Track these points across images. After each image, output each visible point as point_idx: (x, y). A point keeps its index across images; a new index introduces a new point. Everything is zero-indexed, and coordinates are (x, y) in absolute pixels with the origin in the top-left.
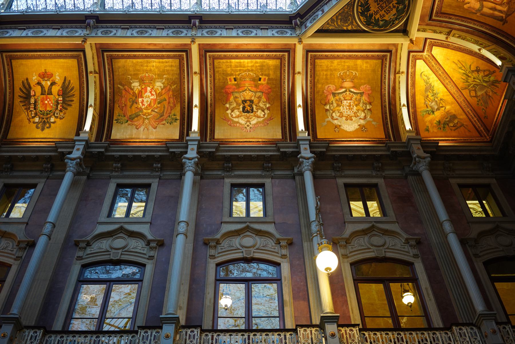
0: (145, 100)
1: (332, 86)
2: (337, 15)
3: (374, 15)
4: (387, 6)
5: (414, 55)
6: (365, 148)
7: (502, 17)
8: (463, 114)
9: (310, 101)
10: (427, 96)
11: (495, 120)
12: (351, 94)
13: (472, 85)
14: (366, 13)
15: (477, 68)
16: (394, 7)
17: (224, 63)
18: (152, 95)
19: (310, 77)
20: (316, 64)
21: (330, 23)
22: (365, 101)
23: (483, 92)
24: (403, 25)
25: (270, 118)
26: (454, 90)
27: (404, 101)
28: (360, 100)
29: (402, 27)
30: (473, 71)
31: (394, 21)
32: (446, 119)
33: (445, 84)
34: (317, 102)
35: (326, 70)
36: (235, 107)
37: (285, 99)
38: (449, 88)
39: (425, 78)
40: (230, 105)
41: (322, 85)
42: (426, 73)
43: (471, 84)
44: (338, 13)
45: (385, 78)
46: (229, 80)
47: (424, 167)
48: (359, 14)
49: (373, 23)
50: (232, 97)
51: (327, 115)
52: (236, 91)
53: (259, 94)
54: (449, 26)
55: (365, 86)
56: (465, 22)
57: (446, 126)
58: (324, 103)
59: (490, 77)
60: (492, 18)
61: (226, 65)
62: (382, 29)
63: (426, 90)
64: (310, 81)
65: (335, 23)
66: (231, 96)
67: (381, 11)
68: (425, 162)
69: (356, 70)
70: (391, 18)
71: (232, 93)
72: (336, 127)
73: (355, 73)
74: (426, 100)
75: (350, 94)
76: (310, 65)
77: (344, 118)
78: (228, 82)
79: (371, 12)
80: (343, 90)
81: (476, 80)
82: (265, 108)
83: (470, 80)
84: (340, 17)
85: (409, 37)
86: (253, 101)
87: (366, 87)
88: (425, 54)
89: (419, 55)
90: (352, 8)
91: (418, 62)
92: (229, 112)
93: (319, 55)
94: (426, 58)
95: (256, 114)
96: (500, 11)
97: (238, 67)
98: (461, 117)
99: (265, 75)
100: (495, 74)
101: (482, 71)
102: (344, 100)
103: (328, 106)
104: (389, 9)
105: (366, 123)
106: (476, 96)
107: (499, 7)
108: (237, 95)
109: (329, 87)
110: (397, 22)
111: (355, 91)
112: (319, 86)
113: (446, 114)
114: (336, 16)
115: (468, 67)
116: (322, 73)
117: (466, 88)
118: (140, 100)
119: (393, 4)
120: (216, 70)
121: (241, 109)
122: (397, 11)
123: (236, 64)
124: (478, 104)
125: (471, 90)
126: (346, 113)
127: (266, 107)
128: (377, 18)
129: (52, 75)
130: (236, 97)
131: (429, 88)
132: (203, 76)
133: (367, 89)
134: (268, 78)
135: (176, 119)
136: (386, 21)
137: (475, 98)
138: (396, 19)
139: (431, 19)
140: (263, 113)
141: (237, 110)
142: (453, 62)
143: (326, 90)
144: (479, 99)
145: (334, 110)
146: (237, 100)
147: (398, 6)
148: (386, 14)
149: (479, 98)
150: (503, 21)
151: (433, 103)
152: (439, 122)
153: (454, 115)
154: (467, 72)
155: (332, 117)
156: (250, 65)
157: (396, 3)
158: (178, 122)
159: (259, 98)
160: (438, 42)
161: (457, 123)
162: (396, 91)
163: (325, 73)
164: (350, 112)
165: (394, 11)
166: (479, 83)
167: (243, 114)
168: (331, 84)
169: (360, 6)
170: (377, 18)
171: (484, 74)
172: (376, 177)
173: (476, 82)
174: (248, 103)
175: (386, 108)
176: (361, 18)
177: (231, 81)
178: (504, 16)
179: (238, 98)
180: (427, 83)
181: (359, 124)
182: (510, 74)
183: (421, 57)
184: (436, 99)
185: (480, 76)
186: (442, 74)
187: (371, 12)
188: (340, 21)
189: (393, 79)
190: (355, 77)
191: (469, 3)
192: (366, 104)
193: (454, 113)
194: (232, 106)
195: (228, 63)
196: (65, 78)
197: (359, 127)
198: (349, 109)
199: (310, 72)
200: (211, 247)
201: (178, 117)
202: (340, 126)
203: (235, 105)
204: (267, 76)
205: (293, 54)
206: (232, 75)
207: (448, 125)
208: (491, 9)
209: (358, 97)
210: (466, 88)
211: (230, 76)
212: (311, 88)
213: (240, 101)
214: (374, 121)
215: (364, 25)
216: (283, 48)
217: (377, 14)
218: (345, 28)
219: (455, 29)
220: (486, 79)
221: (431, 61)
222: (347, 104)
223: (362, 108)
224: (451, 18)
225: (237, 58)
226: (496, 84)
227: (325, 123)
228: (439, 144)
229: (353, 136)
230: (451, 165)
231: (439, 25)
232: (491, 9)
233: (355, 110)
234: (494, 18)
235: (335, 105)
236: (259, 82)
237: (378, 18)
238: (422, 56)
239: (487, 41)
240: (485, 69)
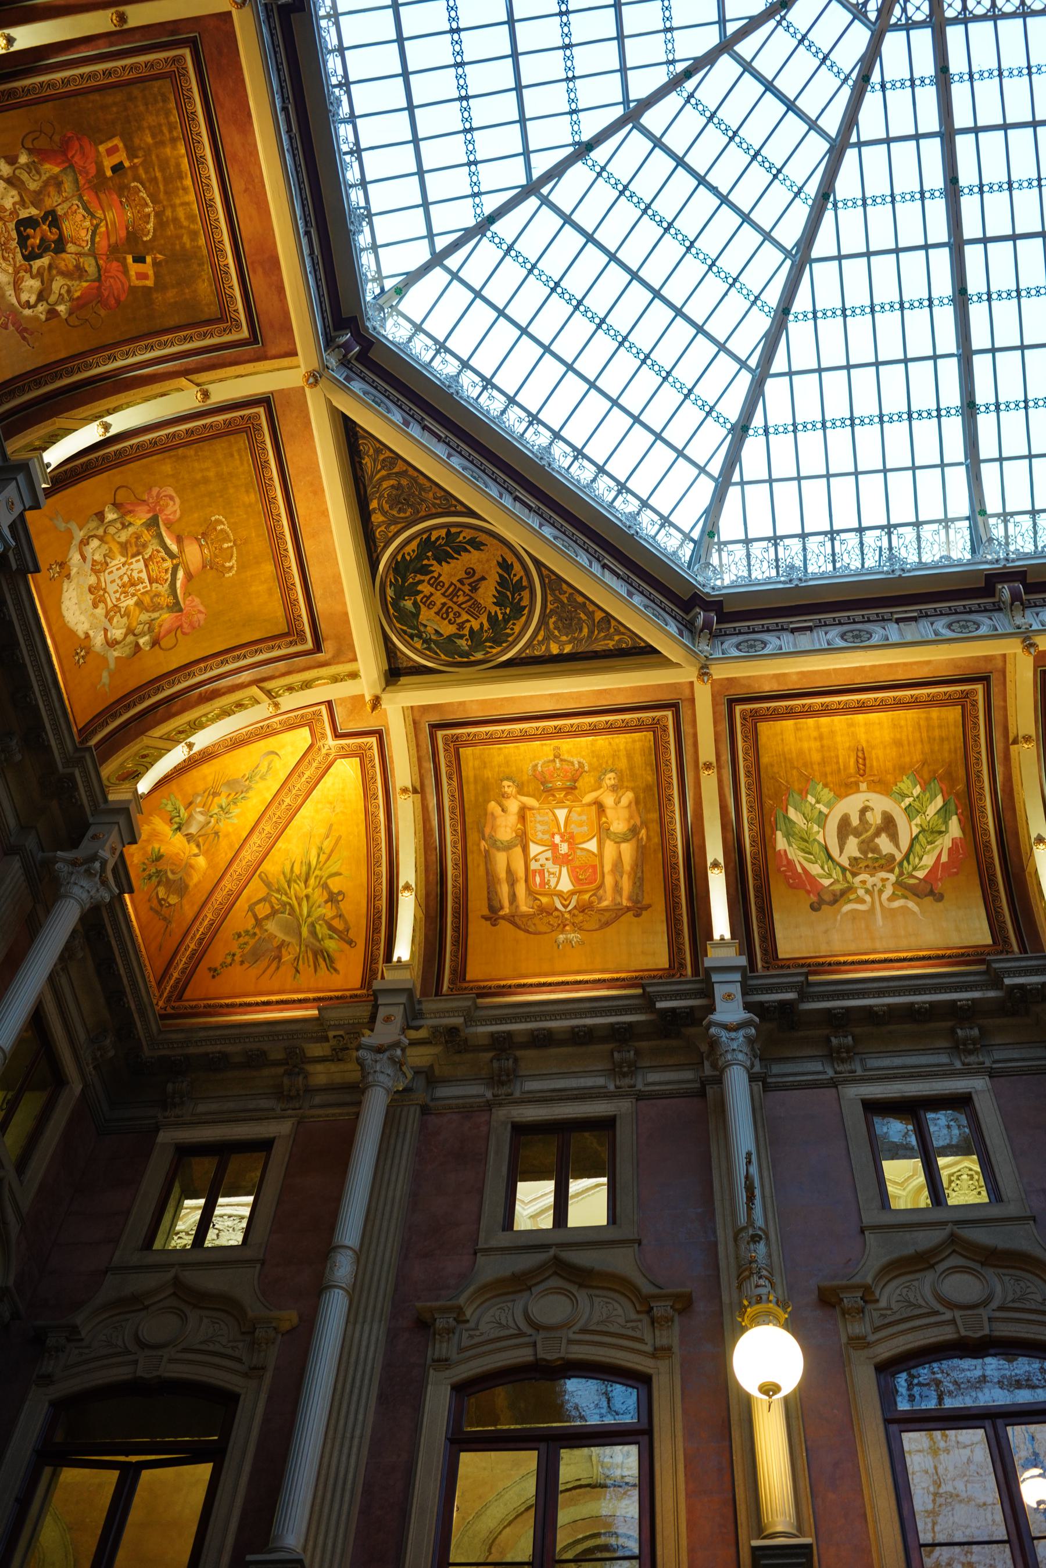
1: (177, 507)
2: (411, 471)
3: (427, 578)
4: (459, 606)
5: (320, 714)
6: (53, 691)
7: (502, 908)
8: (196, 908)
9: (115, 452)
10: (216, 794)
11: (222, 1001)
12: (169, 576)
13: (284, 898)
14: (430, 554)
15: (340, 893)
16: (461, 626)
17: (168, 114)
19: (187, 431)
20: (232, 438)
21: (381, 457)
22: (156, 623)
23: (281, 936)
24: (411, 664)
25: (25, 330)
26: (248, 855)
27: (202, 740)
28: (156, 608)
29: (405, 665)
30: (325, 886)
31: (420, 637)
32: (173, 873)
33: (261, 826)
34: (114, 477)
35: (220, 476)
36: (26, 189)
37: (98, 366)
38: (251, 842)
39: (263, 769)
40: (29, 168)
41: (173, 476)
42: (277, 764)
43: (286, 894)
44: (416, 474)
45: (238, 658)
46: (110, 144)
47: (85, 896)
48: (425, 536)
49: (404, 579)
50: (56, 170)
51: (87, 522)
52: (82, 181)
53: (89, 265)
54: (427, 782)
55: (202, 608)
56: (451, 819)
57: (154, 880)
58: (119, 500)
59: (331, 938)
60: (488, 881)
61: (160, 125)
62: (392, 611)
63: (231, 784)
64: (174, 434)
65: (383, 473)
66: (57, 165)
67: (443, 594)
68: (98, 890)
69: (242, 567)
70: (425, 626)
71: (72, 166)
72: (62, 565)
73: (231, 568)
74: (206, 794)
75: (167, 571)
76: (225, 421)
77: (92, 580)
78: (101, 143)
79: (436, 568)
80: (174, 547)
81: (305, 903)
82: (53, 299)
83: (298, 888)
84: (404, 482)
85: (384, 690)
86: (64, 251)
87: (200, 612)
88: (331, 742)
89: (323, 728)
90: (440, 510)
91: (305, 731)
93: (264, 442)
94: (319, 749)
95: (22, 274)
96: (513, 897)
97: (162, 170)
98: (186, 907)
99: (156, 274)
100: (346, 947)
101: (338, 908)
102: (145, 560)
103: (115, 516)
104: (451, 615)
105: (98, 654)
106: (259, 922)
107: (521, 889)
108: (68, 186)
109: (172, 498)
110: (419, 645)
111: (179, 584)
112: (167, 468)
113: (184, 863)
114: (406, 471)
115: (334, 869)
116: (208, 464)
117: (268, 884)
119: (468, 621)
120: (136, 91)
121: (24, 214)
122: (450, 638)
123: (172, 162)
124: (239, 935)
125: (270, 902)
126: (108, 582)
127: (56, 303)
128: (420, 588)
130: (59, 185)
131: (238, 788)
132: (100, 42)
133: (195, 619)
134: (150, 288)
136: (416, 615)
137: (253, 922)
138: (425, 641)
139: (435, 727)
140: (33, 300)
141: (17, 198)
142: (331, 825)
143: (159, 493)
144: (255, 934)
145: (108, 538)
146: (52, 190)
147: (465, 635)
148: (435, 609)
149: (257, 930)
150: (493, 915)
151: (201, 818)
152: (159, 858)
153: (187, 886)
154: (317, 872)
155: (85, 542)
156: (181, 213)
157: (471, 627)
159: (79, 272)
160: (373, 766)
161: (170, 905)
162: (209, 704)
163: (211, 474)
164: (115, 592)
165: (448, 629)
166: (301, 915)
167: (12, 226)
168: (182, 503)
169: (448, 533)
170: (420, 588)
171: (333, 918)
173: (300, 905)
174: (52, 235)
175: (155, 694)
176: (414, 545)
177: (111, 152)
178: (506, 911)
179: (59, 192)
180: (250, 779)
181: (91, 633)
182: (403, 999)
183: (318, 736)
184: (213, 820)
185: (322, 911)
186: (283, 807)
187: (436, 568)
188: (393, 486)
189: (240, 681)
190: (221, 570)
191: (503, 810)
192: (150, 630)
193: (192, 884)
194: (25, 176)
195: (170, 132)
197: (82, 636)
198: (124, 586)
199: (204, 426)
202: (68, 576)
203: (33, 186)
204: (156, 283)
205: (246, 357)
206: (132, 153)
207: (159, 883)
208: (509, 871)
209: (166, 600)
210: (268, 884)
211: (125, 146)
212: (154, 443)
213: (49, 203)
214: (111, 675)
215: (394, 556)
216: (261, 318)
217: (432, 585)
218: (374, 504)
219: (424, 800)
220: (322, 930)
221: (315, 764)
222: (135, 575)
223: (135, 624)
224: (450, 778)
225: (196, 162)
226: (321, 960)
227: (62, 526)
228: (126, 896)
229: (54, 629)
230: (80, 955)
231: (423, 752)
232: (509, 871)
233: (124, 605)
234: (488, 888)
235: (123, 536)
236: (130, 259)
237: (420, 592)
238: (324, 736)
239: (424, 892)
240: (346, 916)
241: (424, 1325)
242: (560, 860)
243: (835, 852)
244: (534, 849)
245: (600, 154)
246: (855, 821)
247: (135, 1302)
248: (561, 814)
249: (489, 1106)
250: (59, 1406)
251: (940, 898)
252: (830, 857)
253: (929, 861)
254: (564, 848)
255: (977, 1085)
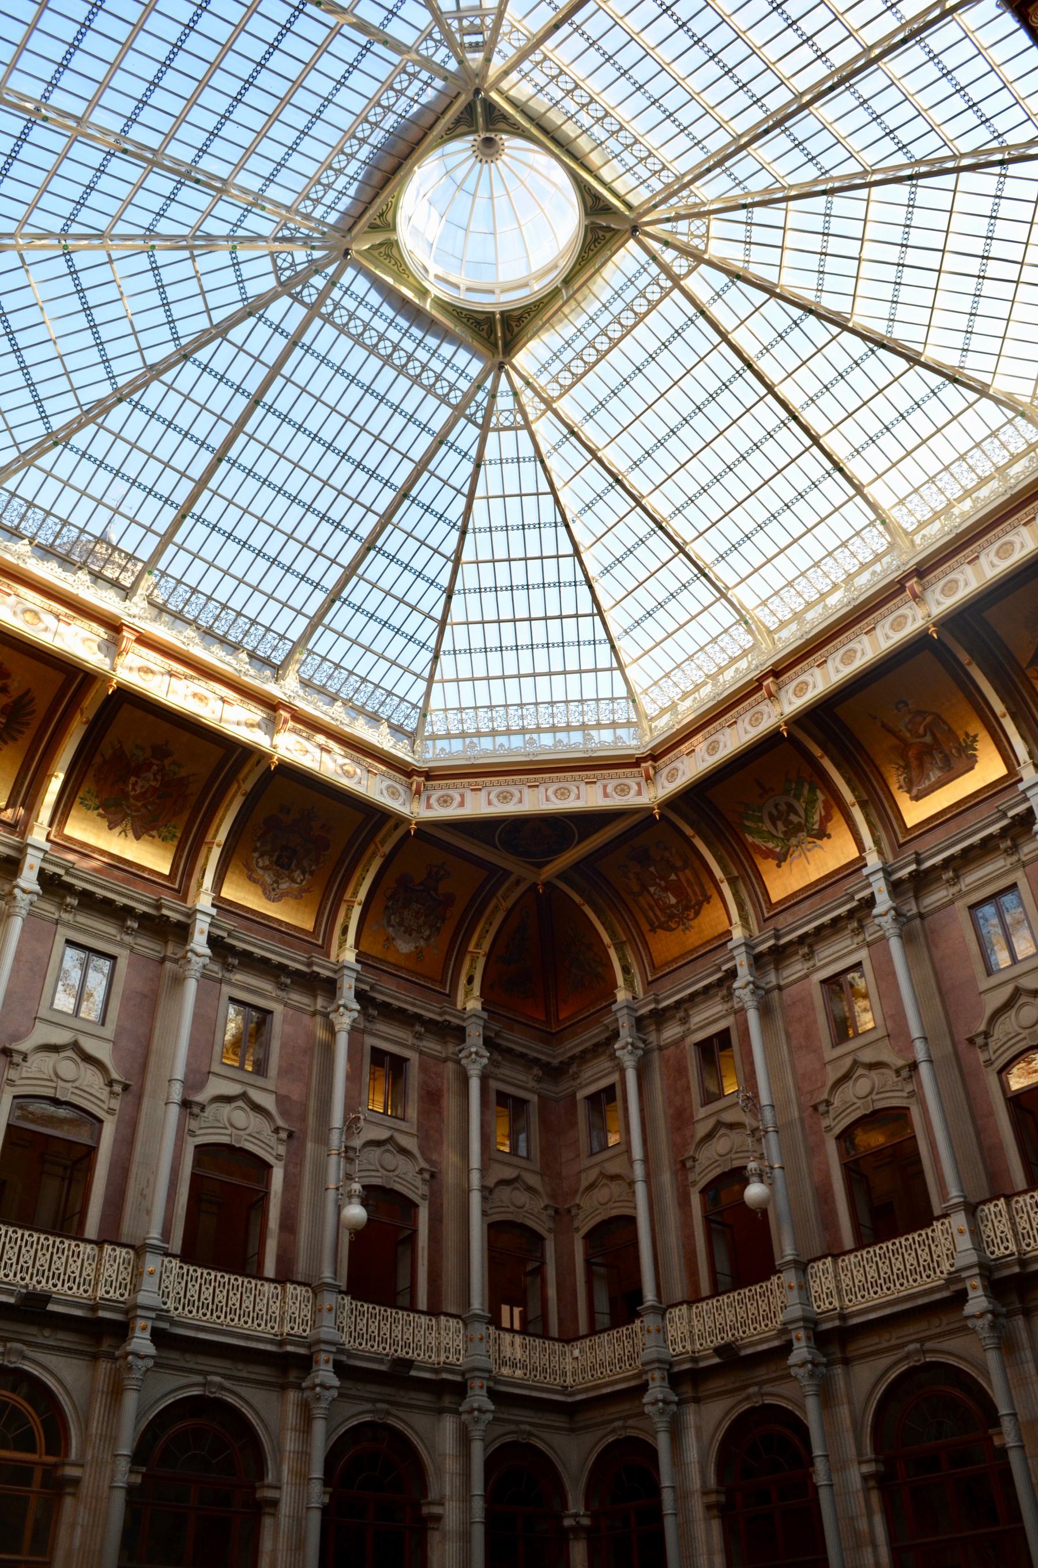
0: (140, 783)
18: (155, 779)
92: (256, 855)
118: (133, 779)
121: (275, 858)
129: (8, 675)
135: (174, 836)
155: (389, 922)
158: (176, 843)
172: (412, 1048)
196: (29, 691)
200: (191, 1114)
201: (179, 835)
241: (683, 1163)
242: (665, 889)
243: (774, 832)
244: (652, 889)
245: (458, 586)
246: (775, 813)
247: (592, 1186)
248: (652, 869)
249: (683, 1038)
250: (586, 1237)
251: (829, 836)
252: (774, 836)
253: (817, 818)
254: (663, 883)
255: (863, 955)
